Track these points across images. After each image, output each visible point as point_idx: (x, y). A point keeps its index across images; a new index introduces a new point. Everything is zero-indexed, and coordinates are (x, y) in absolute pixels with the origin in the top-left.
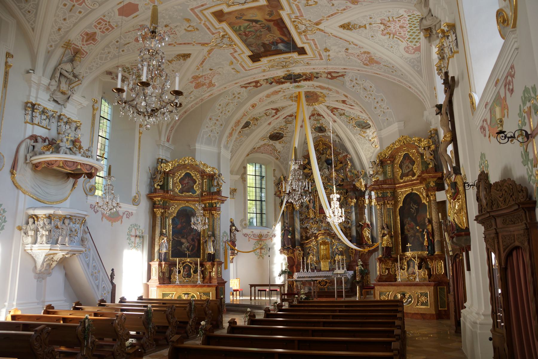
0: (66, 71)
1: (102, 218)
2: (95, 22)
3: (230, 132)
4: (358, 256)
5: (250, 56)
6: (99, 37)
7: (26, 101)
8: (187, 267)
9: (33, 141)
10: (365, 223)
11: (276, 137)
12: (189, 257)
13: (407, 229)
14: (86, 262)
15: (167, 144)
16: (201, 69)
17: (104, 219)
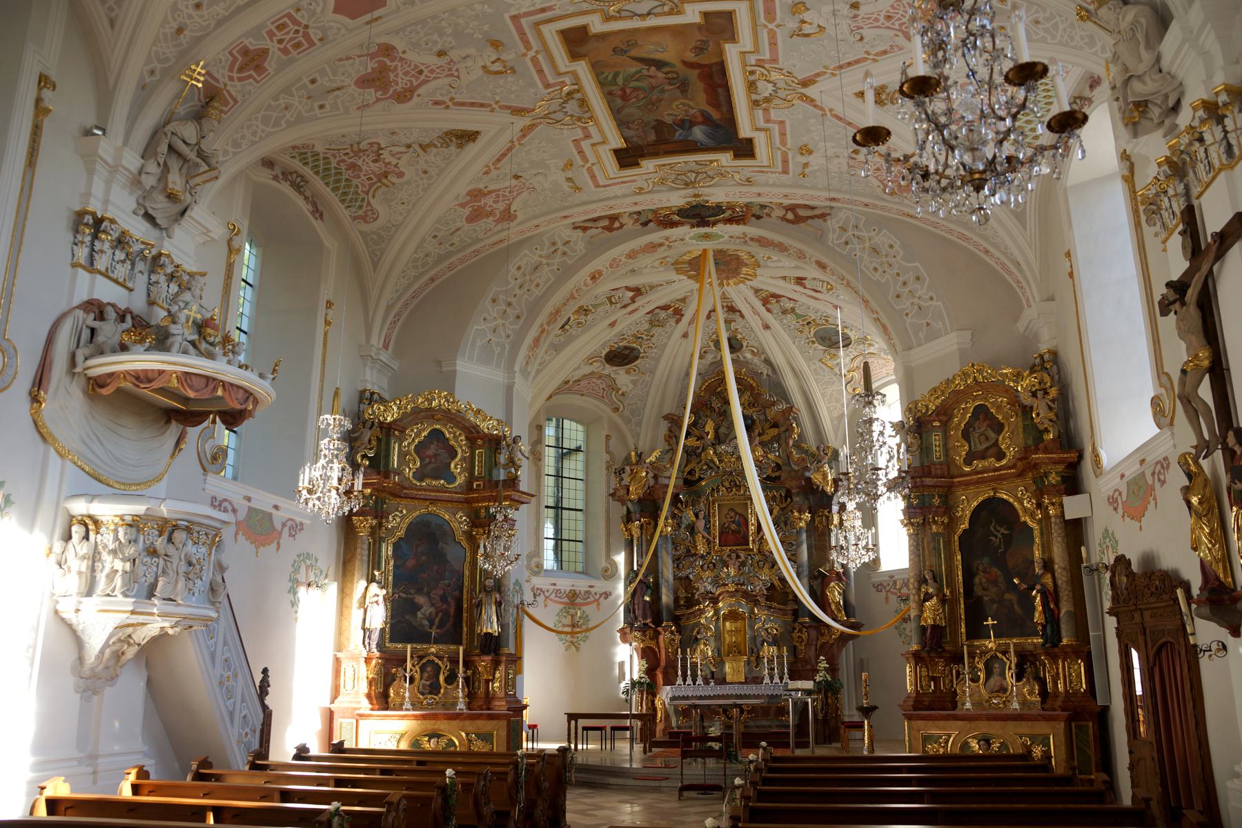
0: (185, 142)
1: (237, 534)
2: (272, 23)
3: (536, 335)
4: (813, 648)
5: (617, 152)
6: (272, 63)
7: (78, 209)
8: (428, 667)
9: (92, 316)
10: (832, 570)
11: (621, 357)
12: (436, 642)
13: (981, 583)
14: (208, 646)
15: (384, 356)
16: (494, 173)
17: (240, 537)
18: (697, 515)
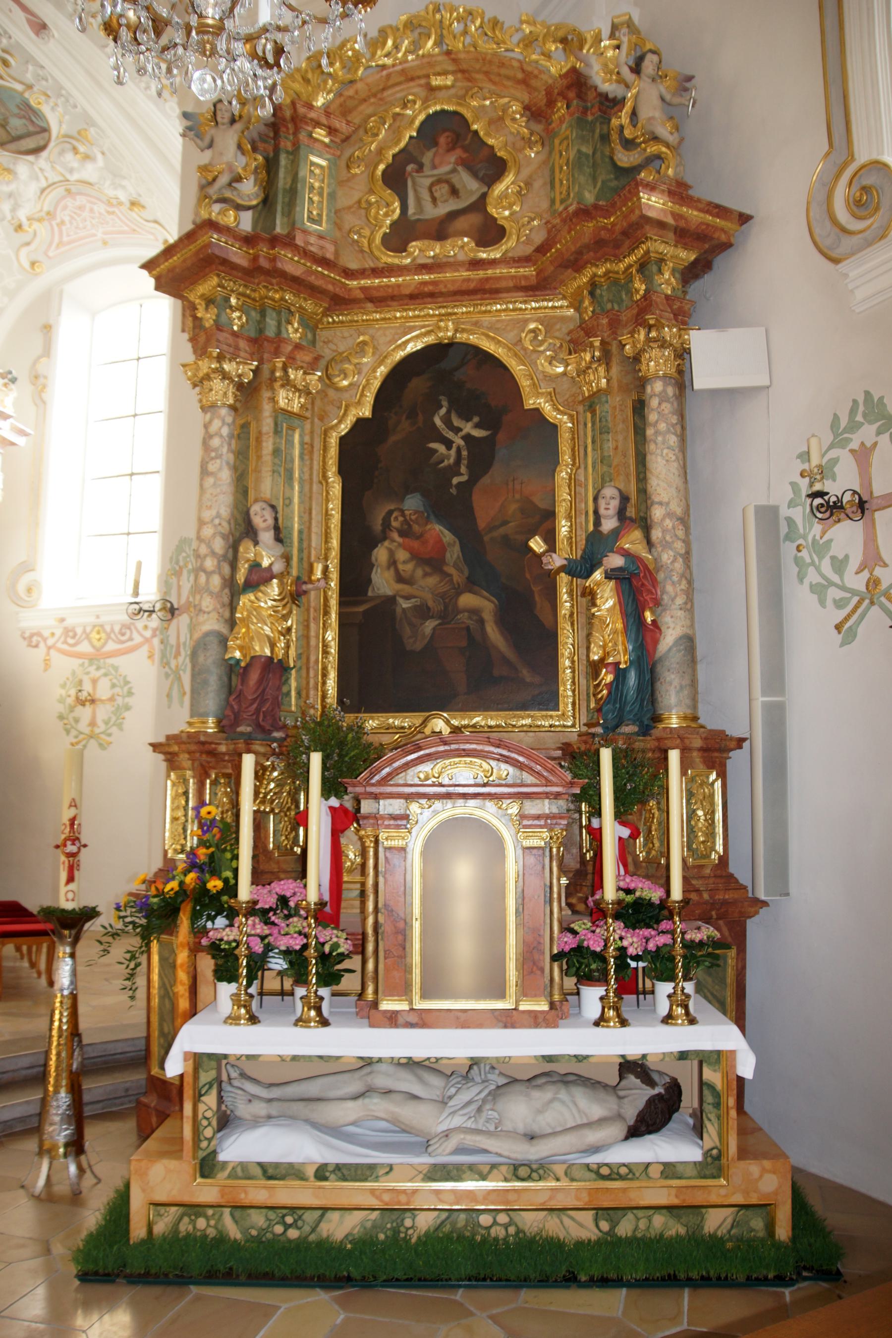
13: (393, 563)
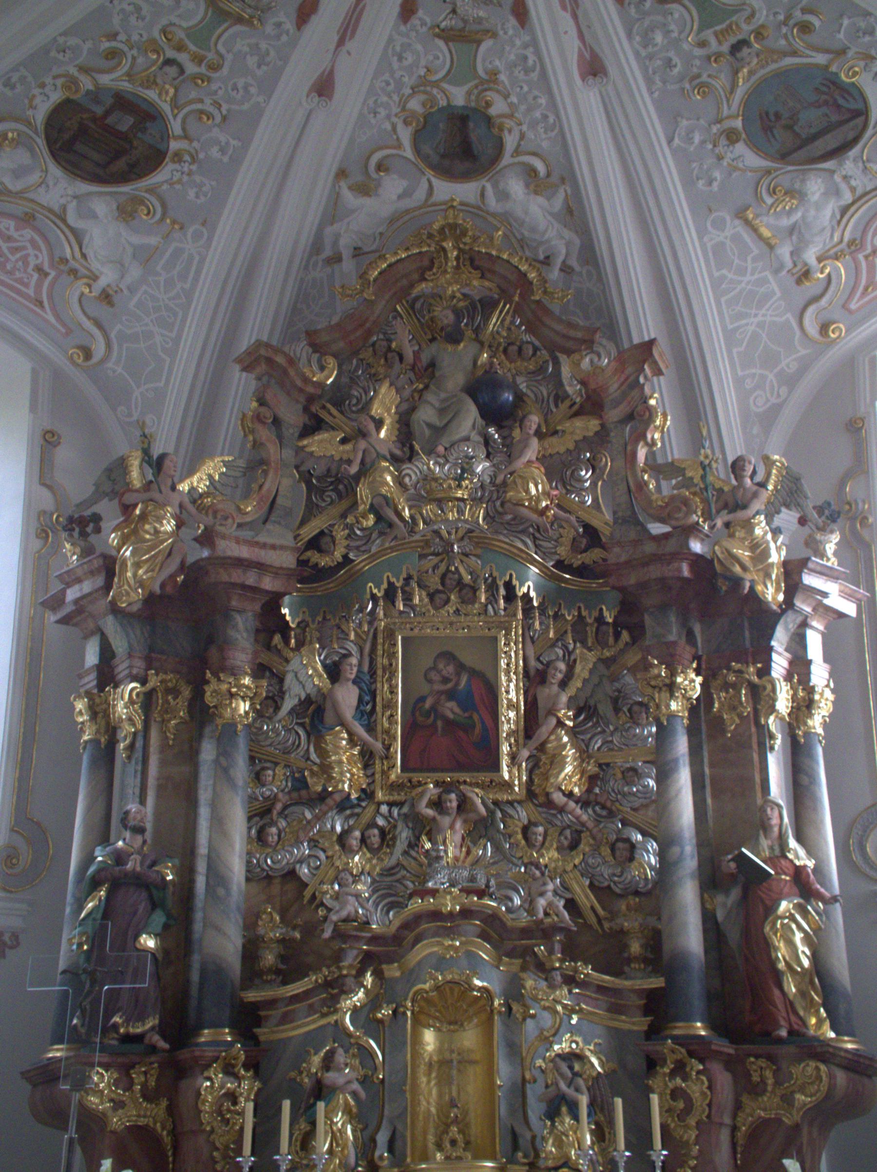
4: (725, 1136)
18: (334, 672)
